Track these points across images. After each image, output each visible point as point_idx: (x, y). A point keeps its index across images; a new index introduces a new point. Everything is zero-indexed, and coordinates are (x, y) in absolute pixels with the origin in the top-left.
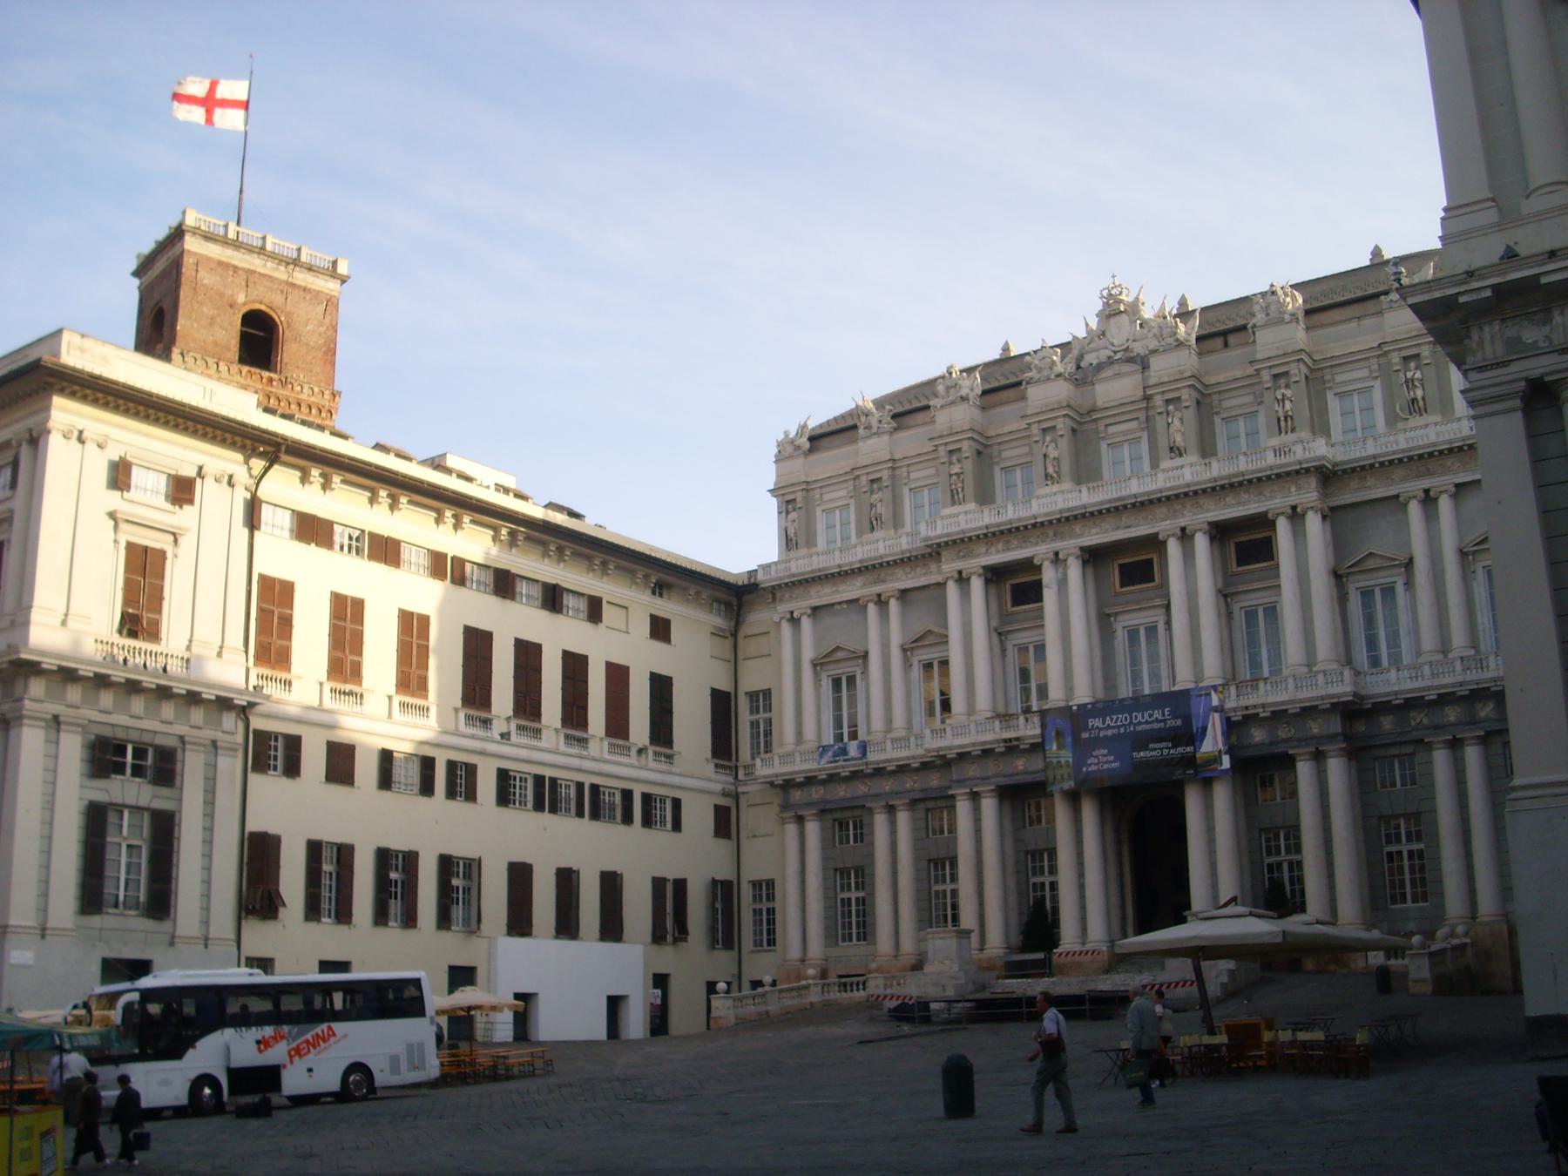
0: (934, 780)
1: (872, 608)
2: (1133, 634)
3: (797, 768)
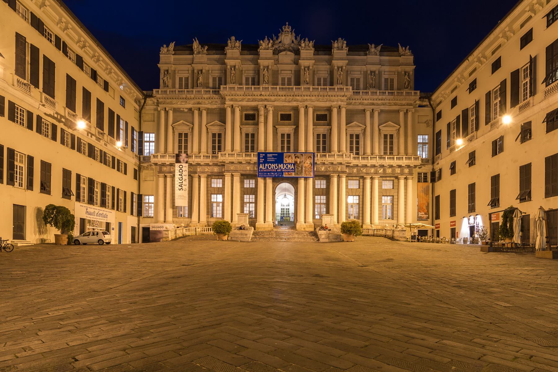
0: (216, 169)
1: (196, 113)
2: (283, 135)
3: (167, 159)
